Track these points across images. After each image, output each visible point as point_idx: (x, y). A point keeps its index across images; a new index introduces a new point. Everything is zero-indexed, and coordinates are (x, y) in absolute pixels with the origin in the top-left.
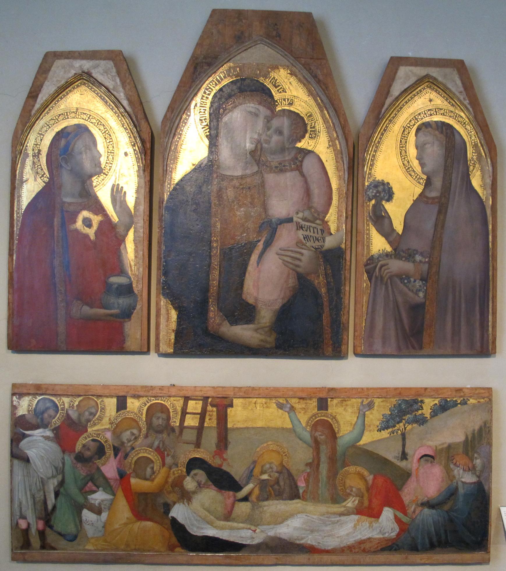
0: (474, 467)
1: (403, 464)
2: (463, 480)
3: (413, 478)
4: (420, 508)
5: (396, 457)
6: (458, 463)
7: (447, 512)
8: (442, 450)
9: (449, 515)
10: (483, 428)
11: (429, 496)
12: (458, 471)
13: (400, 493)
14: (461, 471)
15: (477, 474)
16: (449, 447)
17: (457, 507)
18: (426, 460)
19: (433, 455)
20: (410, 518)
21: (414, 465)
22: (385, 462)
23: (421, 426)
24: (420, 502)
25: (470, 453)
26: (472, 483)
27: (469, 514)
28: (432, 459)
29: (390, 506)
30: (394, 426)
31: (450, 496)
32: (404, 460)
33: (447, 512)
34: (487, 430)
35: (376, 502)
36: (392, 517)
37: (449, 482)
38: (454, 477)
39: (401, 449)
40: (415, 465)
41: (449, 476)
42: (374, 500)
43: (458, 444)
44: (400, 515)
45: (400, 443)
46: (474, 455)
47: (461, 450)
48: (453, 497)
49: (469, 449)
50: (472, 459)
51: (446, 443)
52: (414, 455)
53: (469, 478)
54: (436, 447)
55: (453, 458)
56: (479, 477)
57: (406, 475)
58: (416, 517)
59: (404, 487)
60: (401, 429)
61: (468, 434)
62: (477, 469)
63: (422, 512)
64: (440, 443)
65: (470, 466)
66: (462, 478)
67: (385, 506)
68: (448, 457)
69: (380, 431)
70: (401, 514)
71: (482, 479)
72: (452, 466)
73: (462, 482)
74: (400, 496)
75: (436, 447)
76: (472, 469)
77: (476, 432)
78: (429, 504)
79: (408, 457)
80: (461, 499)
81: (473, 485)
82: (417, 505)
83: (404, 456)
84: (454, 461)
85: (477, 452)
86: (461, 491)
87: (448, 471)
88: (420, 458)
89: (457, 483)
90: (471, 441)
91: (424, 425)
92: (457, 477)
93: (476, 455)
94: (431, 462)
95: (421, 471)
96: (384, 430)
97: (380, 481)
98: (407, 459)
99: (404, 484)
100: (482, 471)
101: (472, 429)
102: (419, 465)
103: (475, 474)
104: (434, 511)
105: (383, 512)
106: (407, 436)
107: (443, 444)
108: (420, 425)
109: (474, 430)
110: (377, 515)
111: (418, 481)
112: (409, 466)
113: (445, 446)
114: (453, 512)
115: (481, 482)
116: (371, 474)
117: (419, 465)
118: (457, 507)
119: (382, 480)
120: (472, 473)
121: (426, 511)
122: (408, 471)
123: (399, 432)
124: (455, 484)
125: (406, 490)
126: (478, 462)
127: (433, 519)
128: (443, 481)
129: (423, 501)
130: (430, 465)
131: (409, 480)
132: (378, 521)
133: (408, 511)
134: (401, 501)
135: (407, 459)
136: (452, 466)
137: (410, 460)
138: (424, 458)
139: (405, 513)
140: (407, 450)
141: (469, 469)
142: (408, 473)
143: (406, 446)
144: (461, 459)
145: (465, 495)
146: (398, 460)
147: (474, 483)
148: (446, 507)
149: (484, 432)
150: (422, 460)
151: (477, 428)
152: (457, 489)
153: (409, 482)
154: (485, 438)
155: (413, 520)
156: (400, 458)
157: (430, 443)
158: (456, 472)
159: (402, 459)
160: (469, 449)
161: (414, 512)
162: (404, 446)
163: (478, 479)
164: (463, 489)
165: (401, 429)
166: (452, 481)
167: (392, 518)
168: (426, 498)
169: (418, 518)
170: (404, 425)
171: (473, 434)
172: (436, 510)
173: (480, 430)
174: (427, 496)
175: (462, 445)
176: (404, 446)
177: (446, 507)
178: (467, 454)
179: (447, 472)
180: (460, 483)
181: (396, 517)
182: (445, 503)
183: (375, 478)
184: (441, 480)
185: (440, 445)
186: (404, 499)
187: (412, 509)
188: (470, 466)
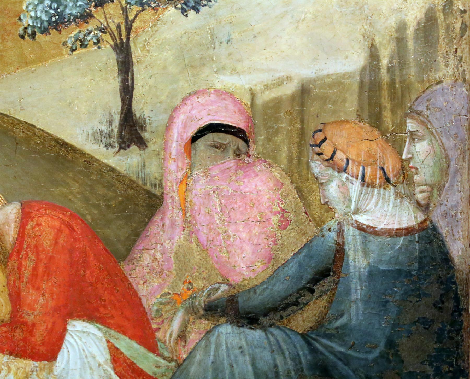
0: (405, 173)
1: (127, 162)
2: (363, 219)
3: (171, 212)
4: (205, 324)
5: (99, 137)
6: (340, 155)
7: (304, 336)
8: (276, 104)
9: (313, 350)
10: (441, 17)
11: (235, 279)
12: (343, 185)
13: (125, 267)
14: (355, 188)
15: (419, 196)
16: (304, 92)
17: (343, 320)
18: (217, 147)
19: (242, 126)
20: (171, 360)
21: (172, 166)
22: (61, 154)
23: (192, 13)
24: (201, 300)
25: (388, 119)
26: (398, 233)
27: (390, 344)
28: (241, 143)
29: (91, 316)
30: (86, 17)
31: (316, 280)
32: (134, 147)
33: (304, 336)
34: (458, 25)
35: (39, 304)
36: (102, 356)
37: (312, 229)
38: (328, 208)
39: (116, 105)
40: (174, 169)
41: (307, 205)
42: (30, 295)
43: (338, 83)
44: (129, 347)
45: (114, 83)
46: (403, 124)
47: (351, 104)
48: (327, 283)
49: (386, 103)
50: (396, 140)
51: (289, 78)
52: (168, 128)
53: (388, 213)
54: (253, 95)
55: (320, 136)
56: (424, 207)
57: (144, 203)
58: (191, 354)
59: (140, 245)
60: (113, 27)
61: (377, 40)
62: (416, 178)
63: (213, 339)
64: (266, 78)
65: (391, 165)
66: (356, 212)
67: (72, 315)
68: (302, 133)
69: (33, 35)
70: (135, 345)
71: (436, 216)
72: (317, 167)
73: (361, 228)
74: (124, 279)
75: (253, 95)
76: (399, 178)
77: (410, 31)
78: (235, 310)
79: (146, 135)
80: (357, 291)
81: (401, 240)
82: (191, 310)
83: (131, 131)
84: (327, 149)
85: (415, 113)
86: (357, 261)
87: (303, 185)
88: (194, 139)
89: (340, 233)
90: (390, 69)
91: (203, 10)
92: (340, 208)
93: (411, 125)
94: (238, 153)
95: (200, 186)
96: (44, 31)
97: (47, 227)
98: (142, 143)
99: (136, 235)
100: (437, 188)
101: (392, 22)
102: (191, 167)
103: (411, 196)
104: (256, 335)
105: (68, 337)
106: (137, 52)
107: (280, 83)
108: (184, 11)
109: (402, 27)
110: (49, 351)
111: (189, 225)
112: (153, 170)
113: (290, 89)
114: (329, 336)
115: (434, 229)
116: (9, 202)
117: (191, 167)
118: (338, 323)
119: (56, 223)
120: (397, 195)
121: (227, 332)
122: (148, 187)
123: (106, 37)
124: (333, 235)
125: (147, 259)
126: (420, 151)
127: (253, 365)
128: (284, 224)
129: (213, 297)
130: (231, 163)
131: (157, 218)
132: (51, 371)
133: (159, 335)
134: (133, 300)
135: (142, 143)
136: (317, 167)
137: (152, 147)
138: (211, 137)
139: (148, 341)
140: (140, 108)
141: (388, 180)
142: (150, 195)
143: (136, 93)
144: (352, 141)
145: (373, 274)
146: (108, 146)
147: (408, 231)
148: (304, 320)
149: (442, 31)
150: (200, 143)
151: (414, 15)
152: (340, 251)
153: (153, 229)
154: (446, 57)
155: (179, 366)
156: (115, 140)
157: (226, 81)
158: (333, 190)
159: (124, 144)
160: (386, 103)
161: (182, 336)
162: (127, 91)
163: (421, 217)
164: (366, 254)
165: (113, 27)
166: (319, 223)
167: (101, 360)
168: (224, 287)
169: (198, 357)
170: (124, 10)
171: (400, 41)
172: (264, 329)
173: (428, 26)
174: (226, 281)
175: (356, 87)
176: (127, 91)
177: (304, 320)
178: (376, 121)
179: (299, 190)
180: (351, 234)
181: (116, 356)
182: (296, 304)
183: (25, 216)
184: (275, 219)
185: (267, 87)
186: (142, 290)
187: (176, 326)
188: (391, 165)
